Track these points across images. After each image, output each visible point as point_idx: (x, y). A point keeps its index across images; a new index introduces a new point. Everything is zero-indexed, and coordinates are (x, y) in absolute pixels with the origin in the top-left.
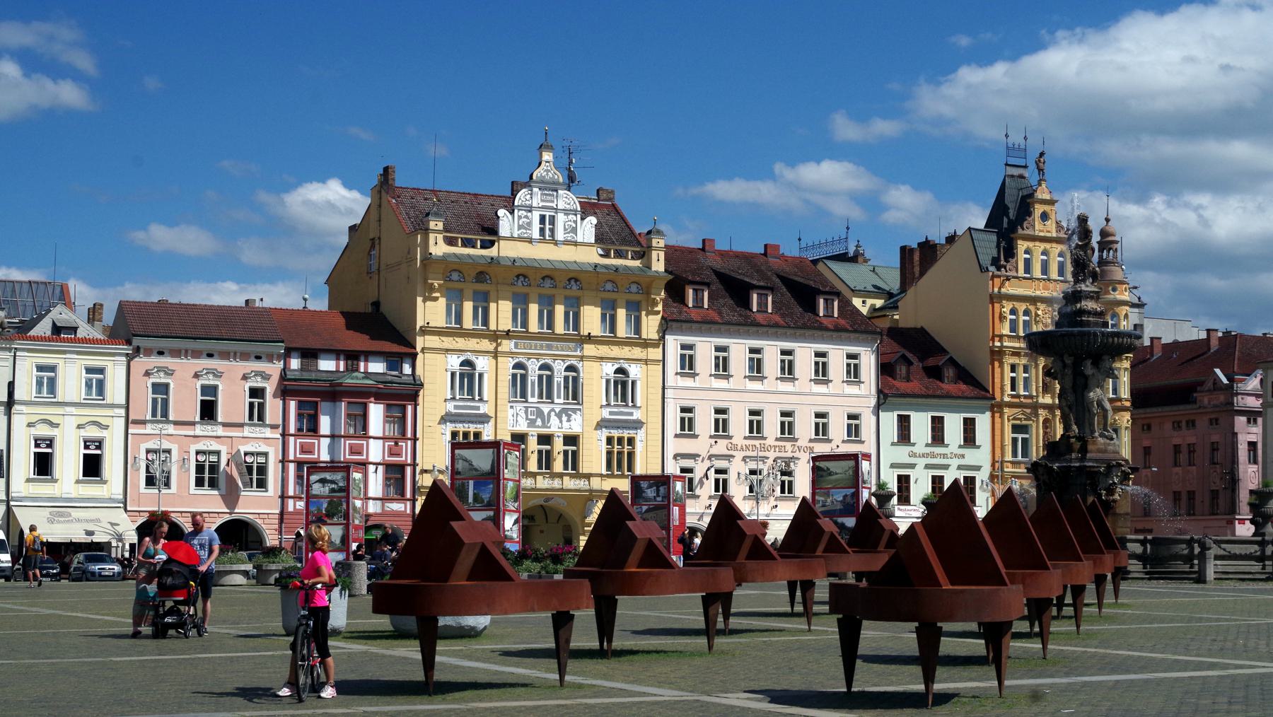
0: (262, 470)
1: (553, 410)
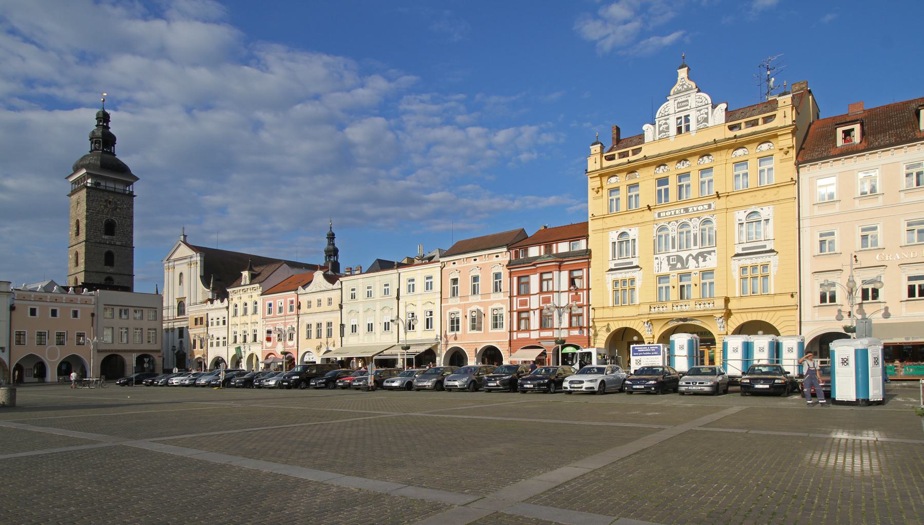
0: (501, 316)
1: (691, 255)
